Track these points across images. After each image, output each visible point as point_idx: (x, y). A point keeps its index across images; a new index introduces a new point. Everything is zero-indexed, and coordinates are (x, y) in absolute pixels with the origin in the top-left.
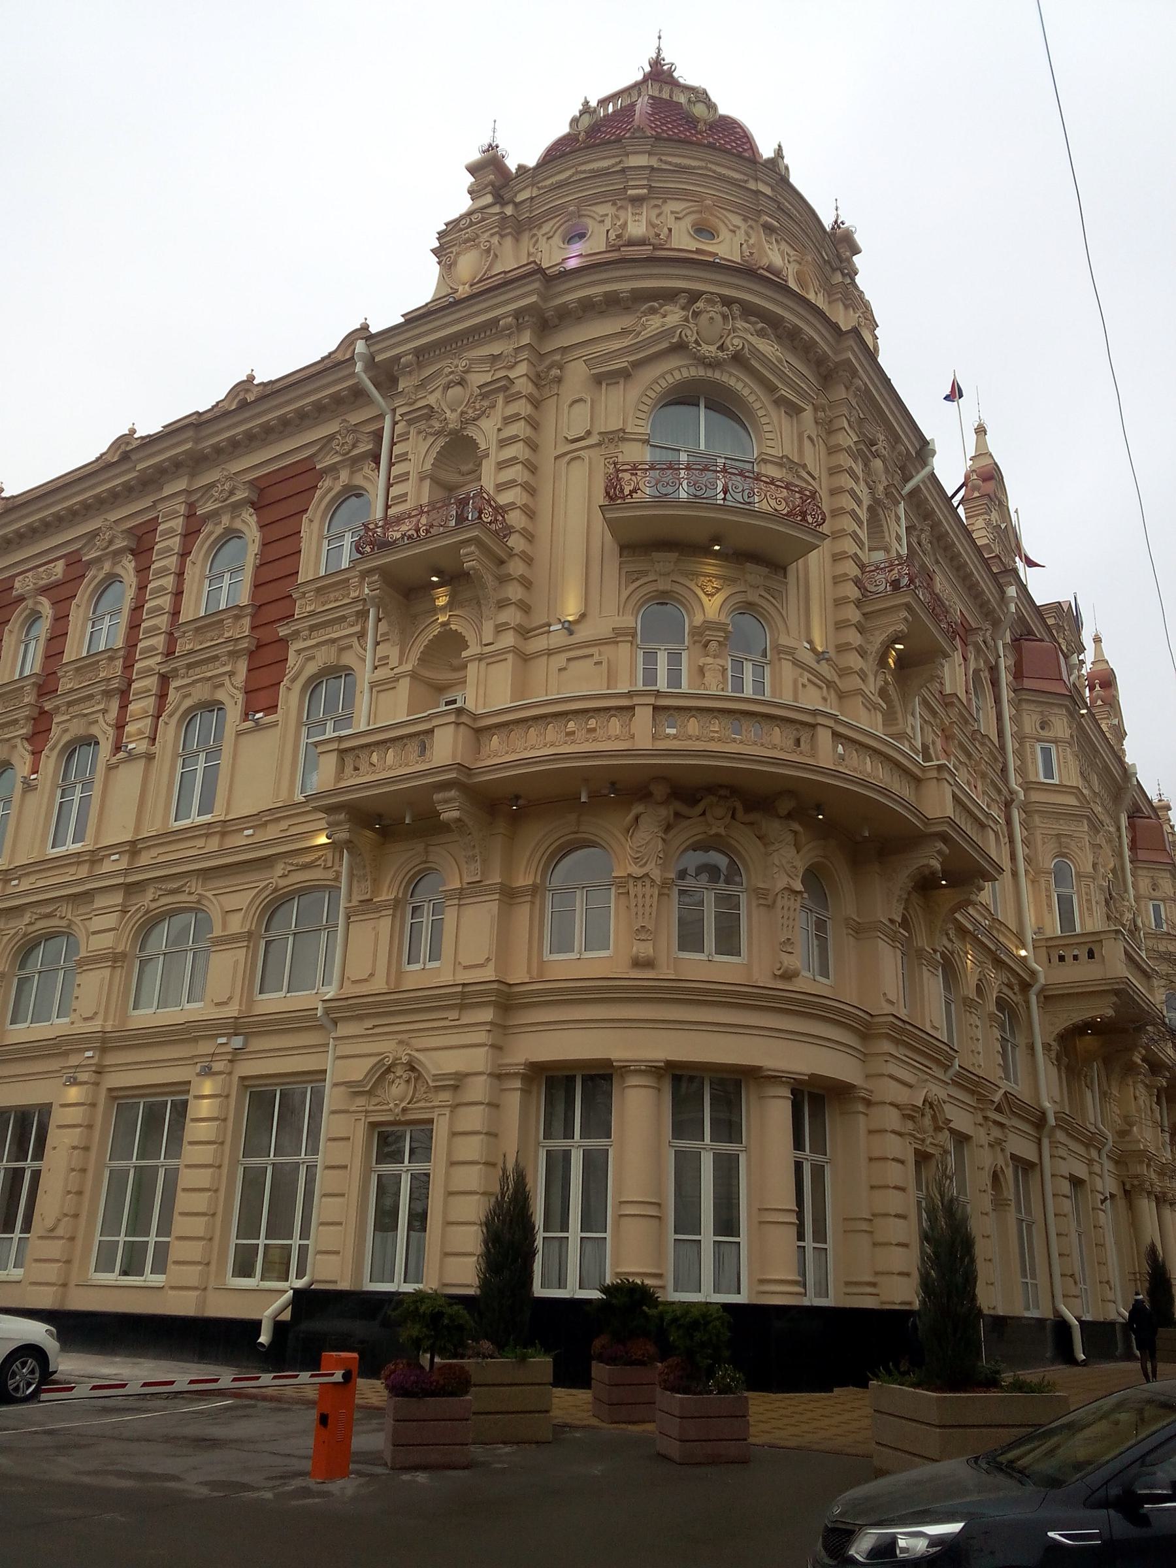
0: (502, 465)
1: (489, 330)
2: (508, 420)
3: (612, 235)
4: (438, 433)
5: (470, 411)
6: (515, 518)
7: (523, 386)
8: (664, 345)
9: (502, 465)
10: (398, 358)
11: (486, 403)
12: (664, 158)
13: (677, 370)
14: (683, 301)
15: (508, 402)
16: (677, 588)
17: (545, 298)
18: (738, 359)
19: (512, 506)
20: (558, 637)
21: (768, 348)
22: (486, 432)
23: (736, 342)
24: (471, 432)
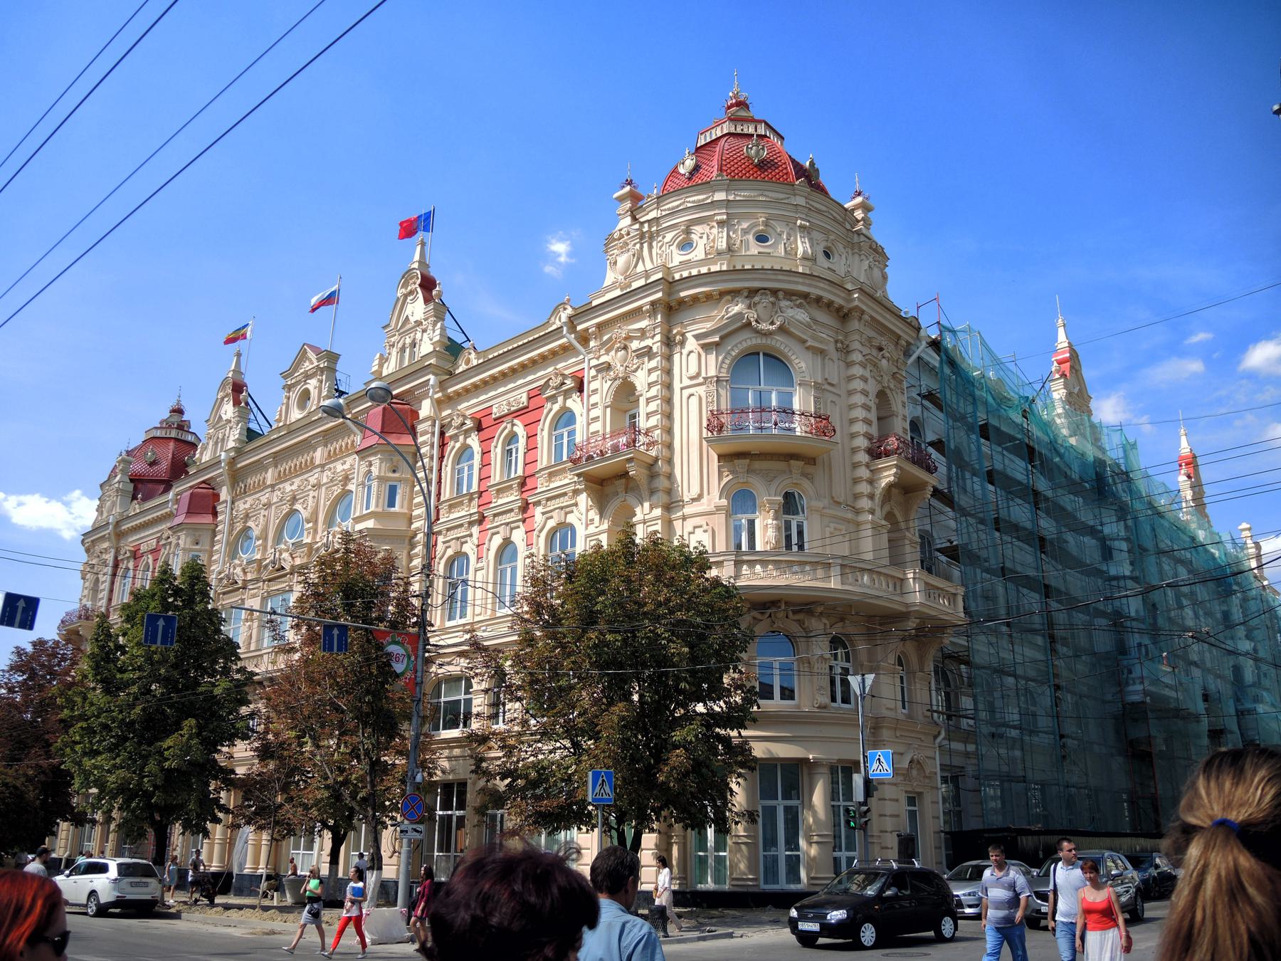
1: (636, 314)
2: (650, 371)
8: (739, 324)
9: (648, 401)
13: (747, 341)
14: (746, 294)
15: (650, 360)
21: (801, 315)
22: (640, 380)
24: (632, 379)
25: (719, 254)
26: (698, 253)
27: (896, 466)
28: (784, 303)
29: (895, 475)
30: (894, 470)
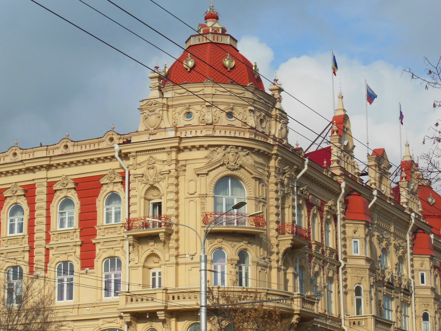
0: (168, 200)
3: (201, 119)
4: (146, 184)
5: (157, 178)
6: (173, 220)
7: (173, 173)
8: (219, 165)
9: (168, 200)
10: (130, 153)
11: (162, 176)
12: (217, 88)
14: (224, 148)
16: (223, 246)
17: (179, 143)
18: (241, 166)
19: (171, 215)
20: (188, 260)
22: (162, 186)
23: (240, 162)
24: (156, 185)
25: (207, 124)
27: (292, 240)
28: (242, 154)
29: (291, 244)
30: (291, 242)
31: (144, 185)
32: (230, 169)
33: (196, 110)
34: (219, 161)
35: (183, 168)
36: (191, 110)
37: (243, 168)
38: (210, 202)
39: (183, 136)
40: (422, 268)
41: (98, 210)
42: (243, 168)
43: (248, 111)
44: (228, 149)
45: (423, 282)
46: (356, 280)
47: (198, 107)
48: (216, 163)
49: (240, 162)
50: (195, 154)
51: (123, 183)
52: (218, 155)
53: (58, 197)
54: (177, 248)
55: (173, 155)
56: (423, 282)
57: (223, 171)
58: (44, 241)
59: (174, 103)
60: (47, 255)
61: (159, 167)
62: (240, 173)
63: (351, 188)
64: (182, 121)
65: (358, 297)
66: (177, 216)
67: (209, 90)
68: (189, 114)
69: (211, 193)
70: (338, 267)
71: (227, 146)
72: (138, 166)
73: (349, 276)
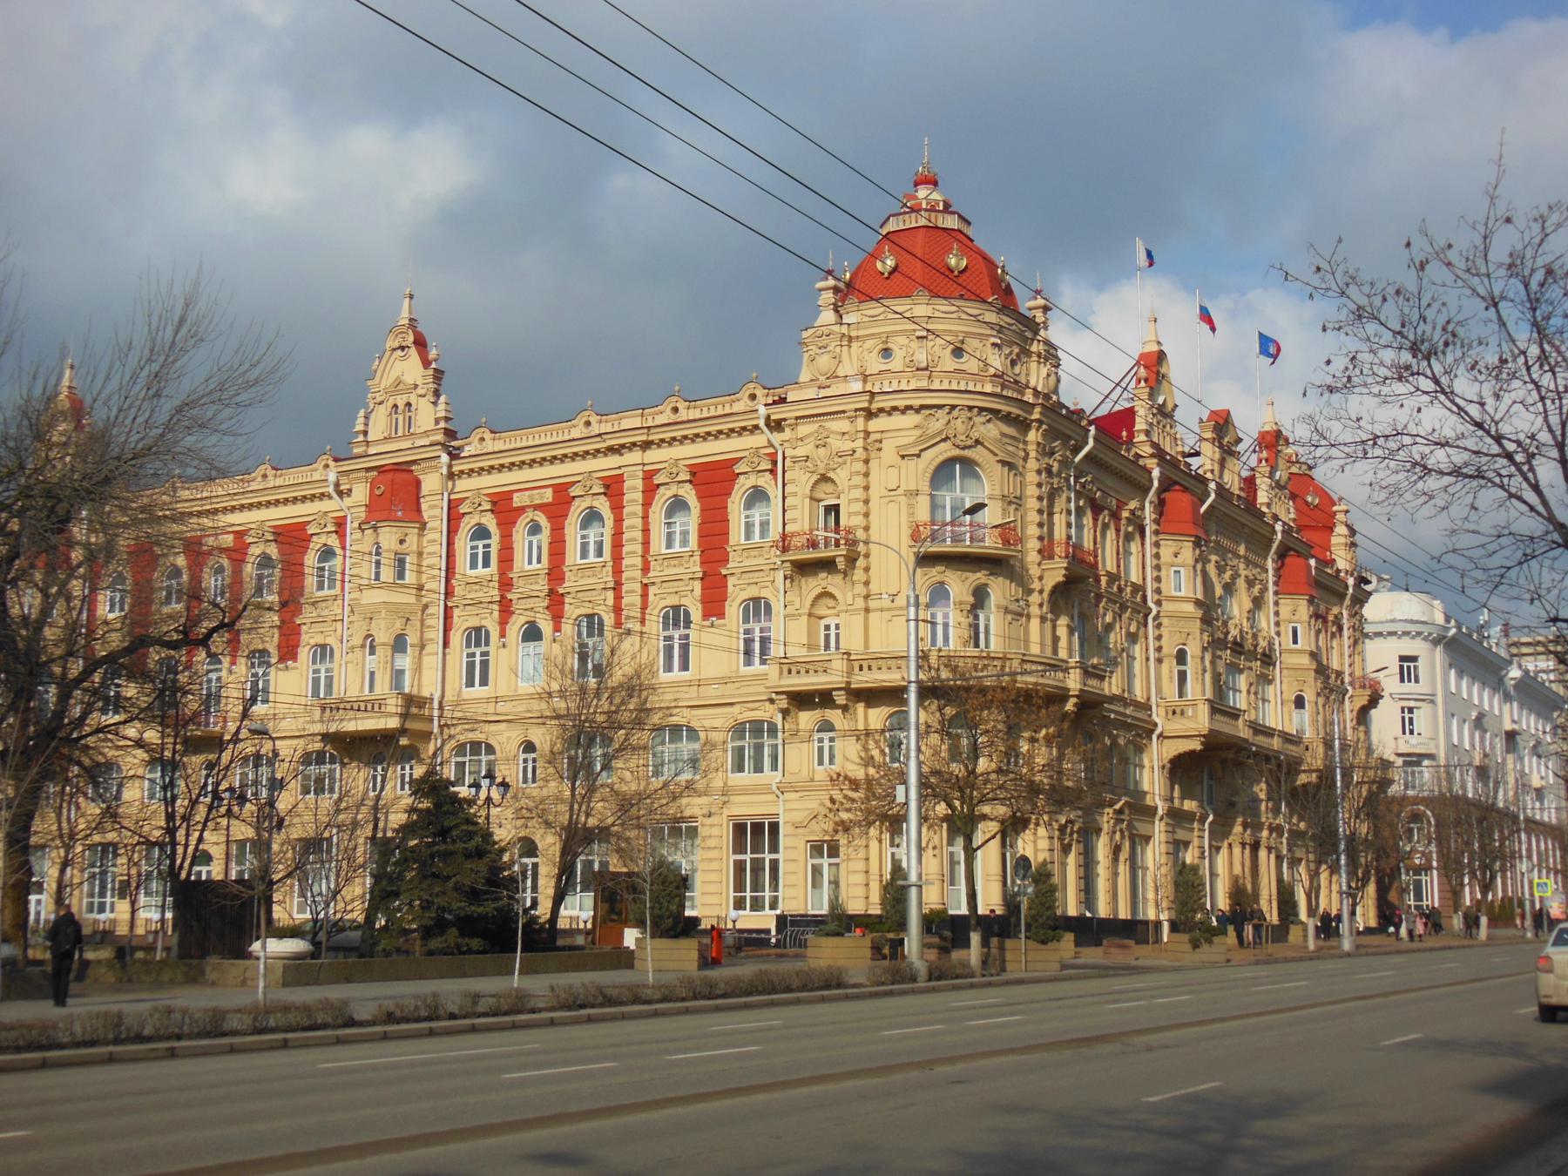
3: (907, 359)
6: (860, 534)
7: (860, 453)
9: (850, 501)
10: (785, 420)
11: (840, 460)
12: (937, 307)
17: (870, 402)
18: (978, 442)
19: (858, 526)
20: (886, 602)
22: (840, 476)
24: (831, 475)
26: (896, 363)
27: (1066, 569)
29: (1065, 575)
30: (1064, 572)
31: (808, 475)
32: (958, 446)
33: (898, 344)
34: (941, 432)
35: (878, 445)
36: (890, 345)
37: (982, 444)
38: (923, 503)
39: (876, 390)
40: (1295, 618)
41: (730, 517)
42: (982, 444)
43: (989, 345)
44: (955, 413)
45: (1295, 641)
46: (1178, 639)
47: (902, 340)
48: (935, 435)
49: (975, 435)
50: (898, 421)
51: (773, 472)
52: (938, 423)
53: (663, 497)
54: (867, 583)
55: (860, 423)
56: (1295, 641)
57: (946, 451)
58: (639, 573)
59: (861, 333)
60: (645, 596)
61: (837, 444)
62: (975, 454)
63: (1169, 478)
64: (875, 364)
65: (1182, 668)
66: (867, 529)
67: (921, 310)
68: (886, 353)
69: (925, 487)
70: (1146, 616)
71: (953, 407)
72: (800, 443)
73: (1164, 631)
